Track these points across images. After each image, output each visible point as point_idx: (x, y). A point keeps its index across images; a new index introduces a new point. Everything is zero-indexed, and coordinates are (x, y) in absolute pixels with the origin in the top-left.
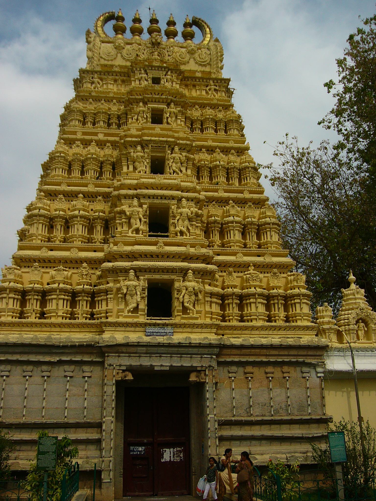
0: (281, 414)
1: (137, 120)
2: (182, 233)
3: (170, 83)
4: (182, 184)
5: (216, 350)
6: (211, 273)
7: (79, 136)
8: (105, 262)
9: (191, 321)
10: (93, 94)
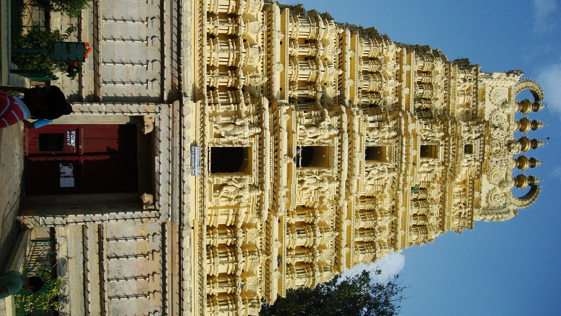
0: (110, 290)
1: (425, 130)
3: (467, 165)
6: (259, 214)
7: (406, 68)
8: (269, 100)
9: (208, 193)
10: (452, 81)
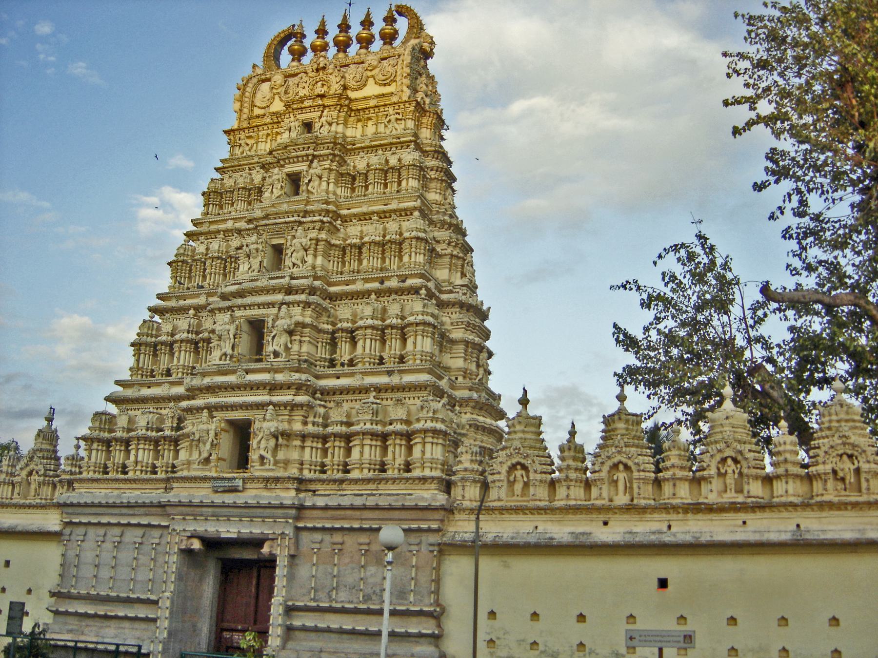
1: (272, 192)
2: (276, 354)
3: (327, 127)
4: (294, 282)
5: (293, 512)
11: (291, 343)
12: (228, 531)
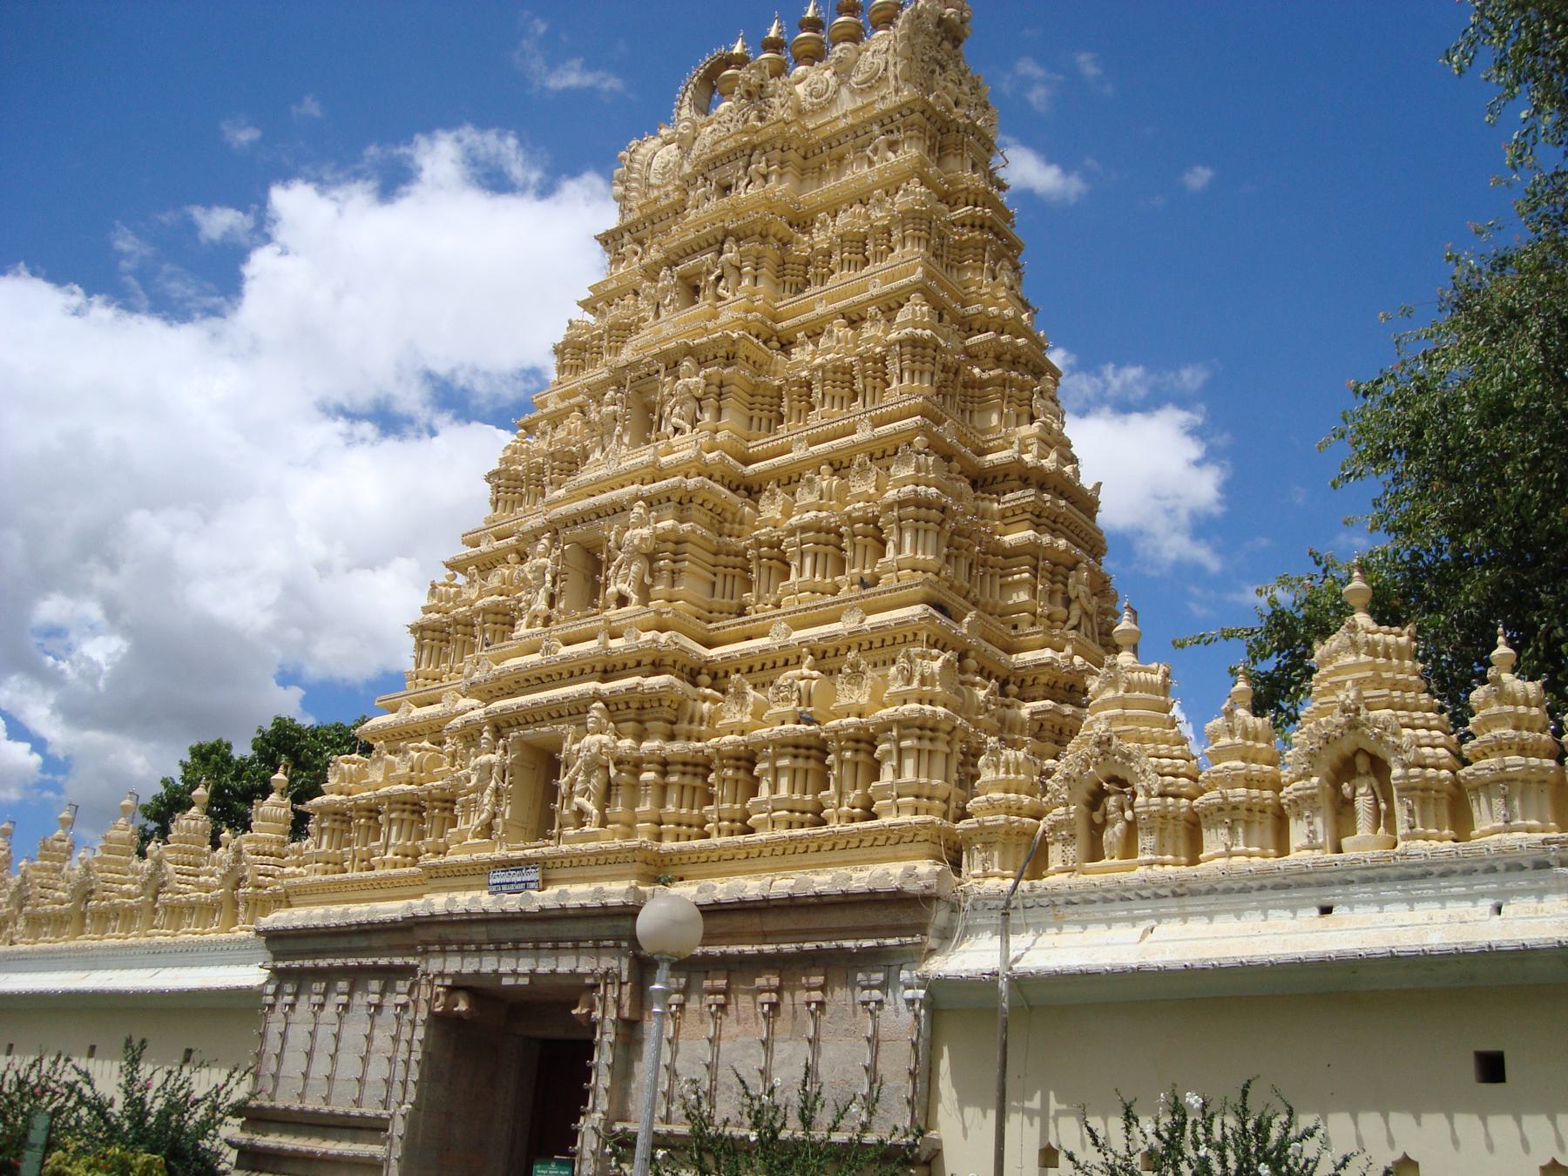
2: (622, 600)
11: (651, 575)
12: (515, 973)
